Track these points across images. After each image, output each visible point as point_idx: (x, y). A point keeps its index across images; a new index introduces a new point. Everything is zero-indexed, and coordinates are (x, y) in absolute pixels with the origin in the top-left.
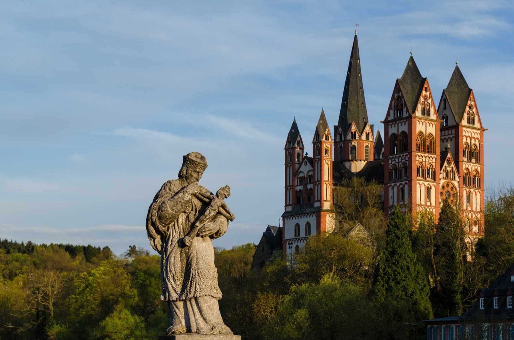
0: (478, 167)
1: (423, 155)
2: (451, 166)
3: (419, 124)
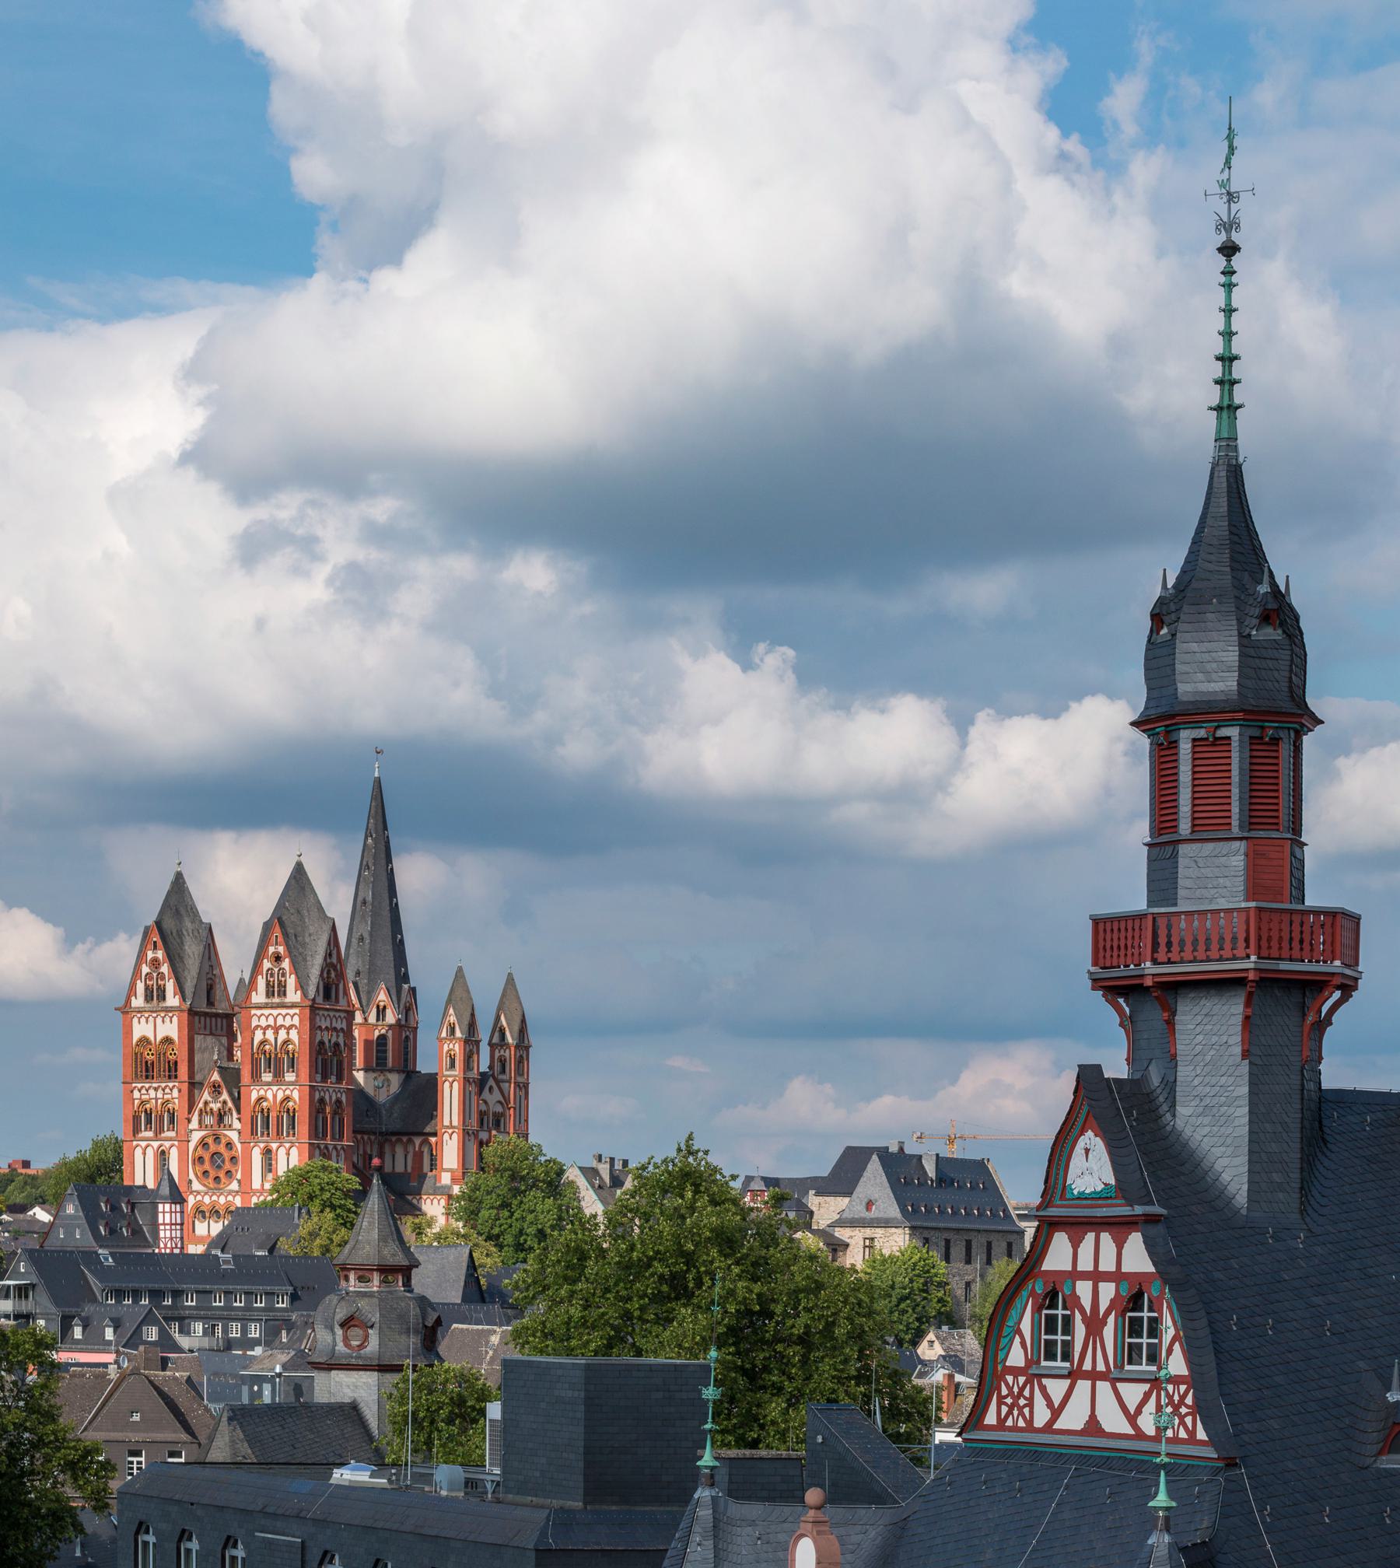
1: (147, 1085)
2: (221, 1099)
3: (139, 1022)
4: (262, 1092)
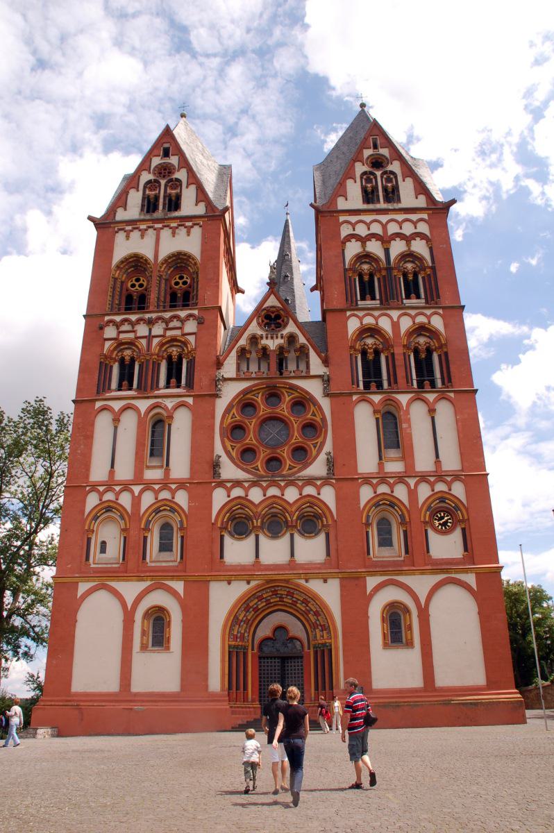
0: (429, 317)
1: (133, 318)
2: (286, 332)
3: (128, 237)
4: (369, 320)
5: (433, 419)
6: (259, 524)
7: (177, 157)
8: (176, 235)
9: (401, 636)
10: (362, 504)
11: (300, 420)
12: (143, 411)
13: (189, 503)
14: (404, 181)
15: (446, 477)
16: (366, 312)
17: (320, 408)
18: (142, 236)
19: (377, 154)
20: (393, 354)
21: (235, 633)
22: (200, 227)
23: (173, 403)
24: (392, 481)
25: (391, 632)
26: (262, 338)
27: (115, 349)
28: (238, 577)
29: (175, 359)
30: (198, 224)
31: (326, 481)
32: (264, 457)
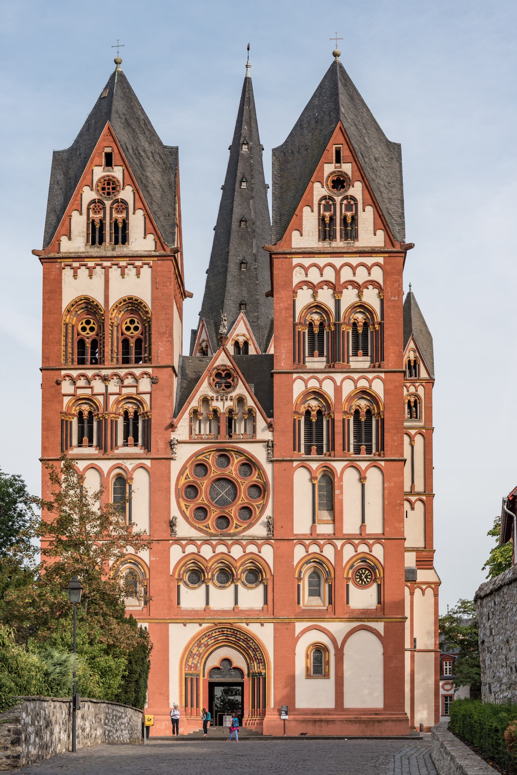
0: (370, 382)
1: (90, 373)
2: (234, 394)
3: (75, 276)
4: (313, 384)
5: (363, 486)
6: (210, 577)
7: (121, 168)
8: (125, 276)
9: (322, 668)
10: (295, 563)
11: (247, 482)
12: (106, 472)
13: (150, 557)
14: (364, 211)
15: (369, 541)
16: (311, 375)
17: (264, 472)
18: (91, 276)
19: (338, 171)
20: (333, 420)
21: (190, 664)
22: (151, 267)
23: (133, 466)
24: (322, 542)
25: (314, 666)
26: (213, 400)
27: (73, 405)
28: (192, 621)
29: (131, 416)
30: (148, 264)
31: (267, 540)
32: (214, 516)
